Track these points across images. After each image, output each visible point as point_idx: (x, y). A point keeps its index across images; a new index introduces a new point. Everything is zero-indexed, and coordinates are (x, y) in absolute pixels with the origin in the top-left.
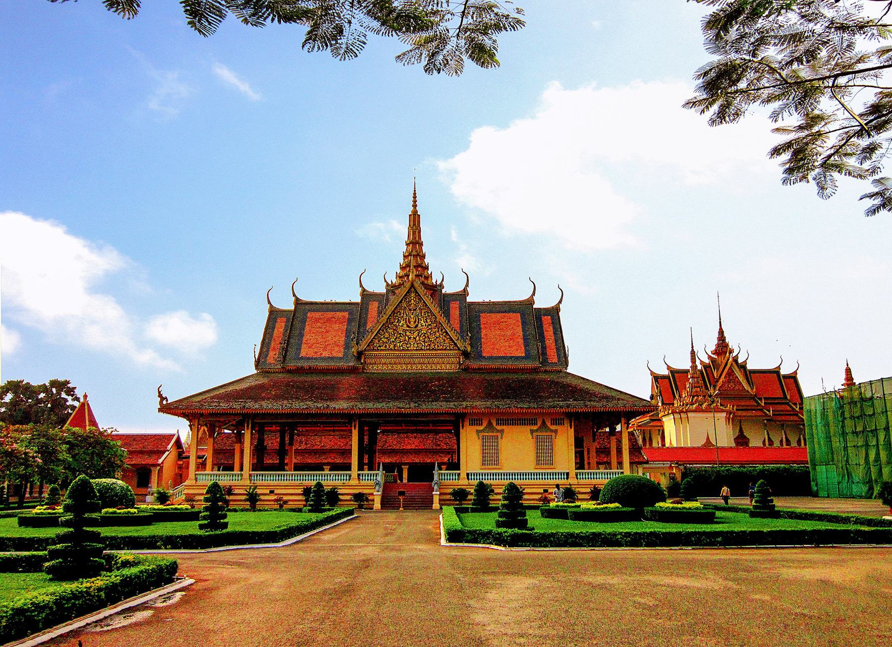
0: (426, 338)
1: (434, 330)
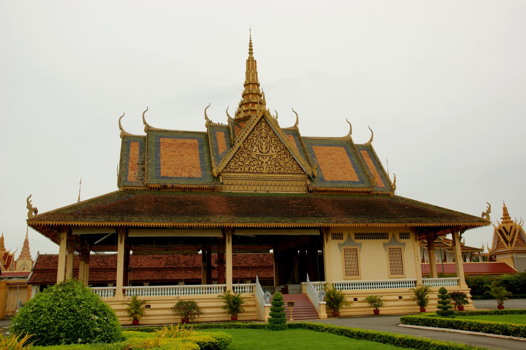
0: (276, 162)
1: (283, 156)
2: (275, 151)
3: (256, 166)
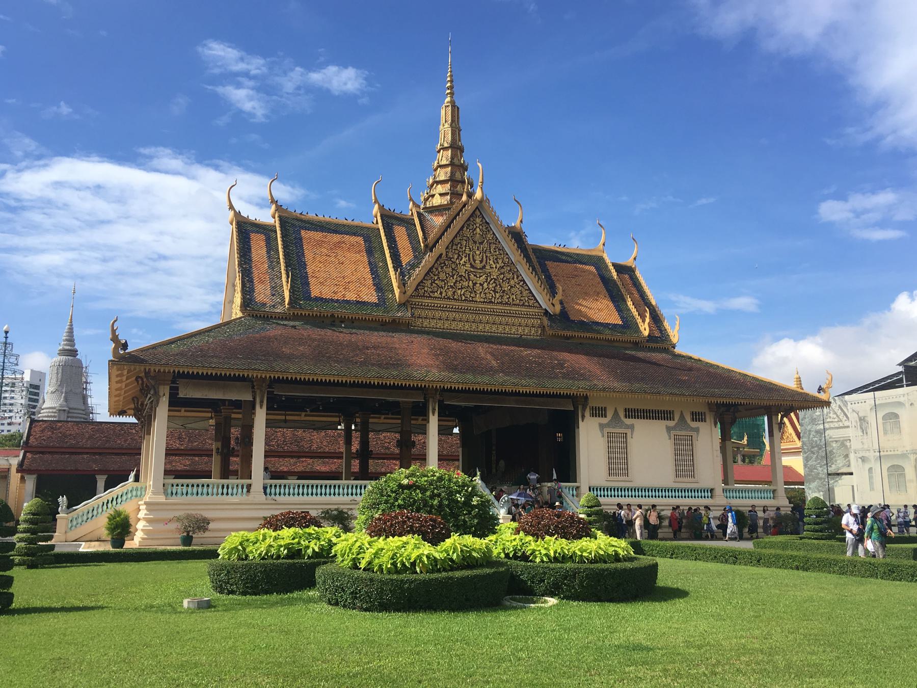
0: (496, 285)
2: (494, 266)
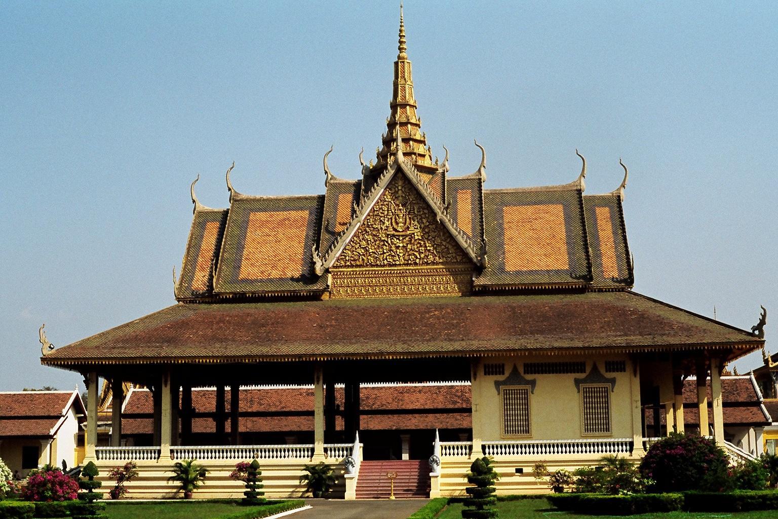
0: (421, 246)
3: (387, 254)
